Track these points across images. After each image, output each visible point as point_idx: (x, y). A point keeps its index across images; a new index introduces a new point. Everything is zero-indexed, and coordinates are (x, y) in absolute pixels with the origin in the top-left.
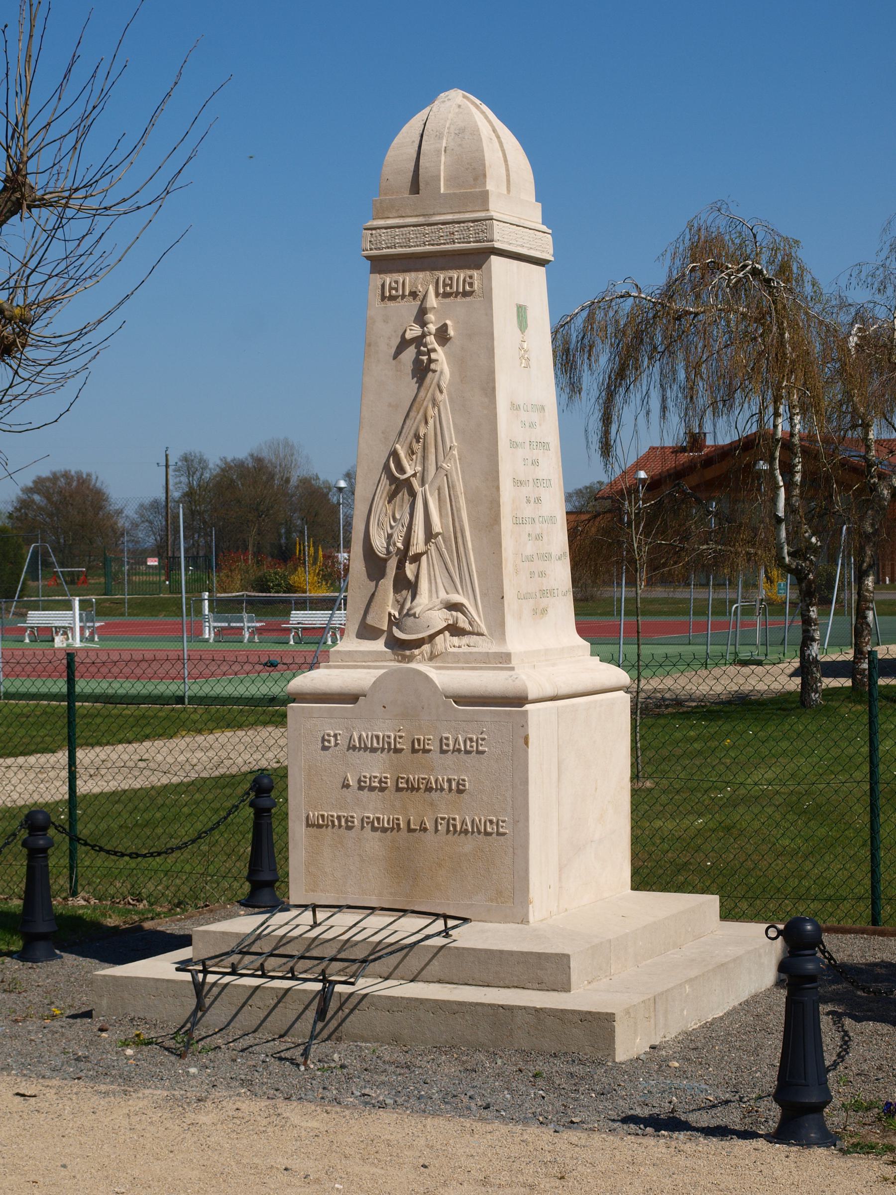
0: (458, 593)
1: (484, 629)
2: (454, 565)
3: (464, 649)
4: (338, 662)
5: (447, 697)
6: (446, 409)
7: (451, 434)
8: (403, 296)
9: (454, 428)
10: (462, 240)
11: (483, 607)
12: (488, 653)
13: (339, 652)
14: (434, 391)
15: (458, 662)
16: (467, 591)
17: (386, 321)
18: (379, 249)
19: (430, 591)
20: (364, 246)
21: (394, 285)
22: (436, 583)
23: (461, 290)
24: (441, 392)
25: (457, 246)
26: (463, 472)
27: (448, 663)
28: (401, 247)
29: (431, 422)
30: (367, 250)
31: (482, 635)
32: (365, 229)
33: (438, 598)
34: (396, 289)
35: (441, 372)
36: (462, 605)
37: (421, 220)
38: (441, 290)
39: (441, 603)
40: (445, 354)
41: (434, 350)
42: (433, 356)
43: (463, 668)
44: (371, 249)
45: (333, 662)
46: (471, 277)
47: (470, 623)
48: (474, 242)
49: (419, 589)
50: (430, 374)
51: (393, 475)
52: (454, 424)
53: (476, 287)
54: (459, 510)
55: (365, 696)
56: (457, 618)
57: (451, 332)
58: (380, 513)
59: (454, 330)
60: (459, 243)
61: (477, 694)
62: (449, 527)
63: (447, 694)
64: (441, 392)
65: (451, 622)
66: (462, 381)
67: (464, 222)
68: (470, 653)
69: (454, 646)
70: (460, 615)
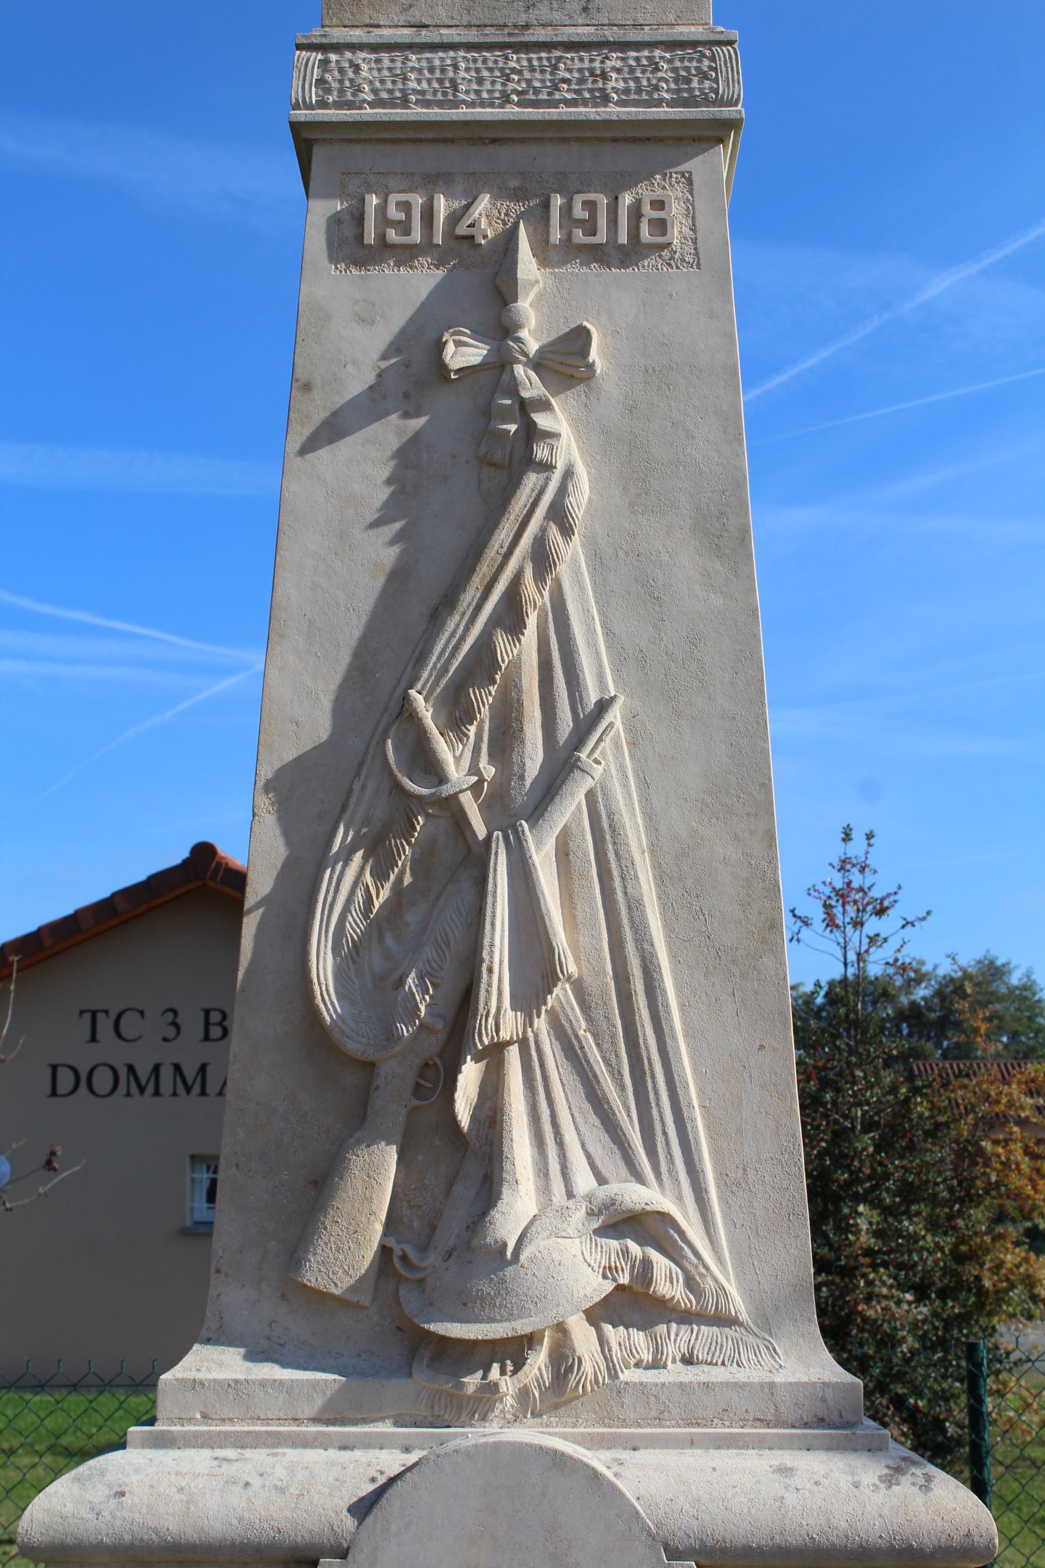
0: (640, 1179)
1: (738, 1304)
2: (622, 1087)
3: (675, 1373)
4: (190, 1420)
5: (674, 1553)
6: (582, 588)
7: (600, 666)
8: (427, 246)
9: (608, 648)
10: (633, 96)
11: (731, 1224)
12: (772, 1385)
13: (195, 1385)
14: (543, 530)
15: (659, 1420)
16: (672, 1171)
17: (365, 320)
18: (350, 105)
19: (543, 1172)
20: (296, 93)
21: (394, 213)
22: (560, 1144)
23: (623, 238)
24: (567, 531)
25: (613, 111)
26: (644, 785)
27: (624, 1423)
28: (427, 104)
29: (532, 621)
30: (310, 107)
31: (724, 1320)
32: (299, 47)
33: (570, 1195)
34: (405, 228)
35: (569, 474)
36: (665, 1218)
37: (493, 36)
38: (556, 235)
39: (591, 1214)
40: (574, 422)
41: (544, 406)
42: (542, 420)
43: (692, 1443)
44: (322, 104)
45: (171, 1421)
46: (659, 205)
47: (690, 1283)
48: (672, 104)
49: (507, 1166)
50: (531, 480)
51: (397, 786)
52: (608, 632)
53: (677, 233)
54: (635, 906)
55: (343, 1554)
56: (647, 1264)
57: (594, 355)
58: (346, 910)
59: (603, 354)
60: (621, 103)
61: (794, 1538)
62: (600, 959)
63: (680, 1542)
64: (567, 531)
65: (624, 1279)
66: (632, 505)
67: (638, 46)
68: (706, 1385)
69: (637, 1365)
70: (655, 1256)
